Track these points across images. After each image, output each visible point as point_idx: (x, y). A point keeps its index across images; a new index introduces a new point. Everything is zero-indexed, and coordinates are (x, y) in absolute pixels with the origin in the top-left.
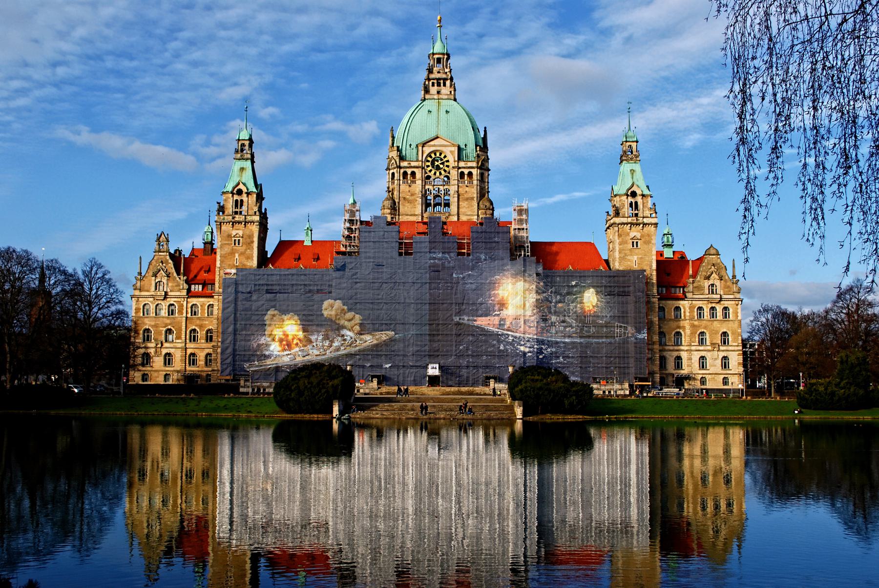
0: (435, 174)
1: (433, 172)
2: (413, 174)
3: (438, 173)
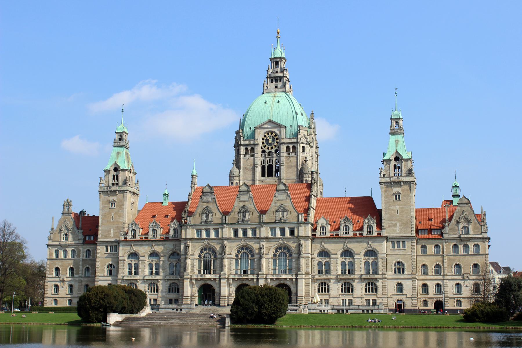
0: (268, 148)
1: (267, 147)
2: (253, 149)
3: (270, 148)
